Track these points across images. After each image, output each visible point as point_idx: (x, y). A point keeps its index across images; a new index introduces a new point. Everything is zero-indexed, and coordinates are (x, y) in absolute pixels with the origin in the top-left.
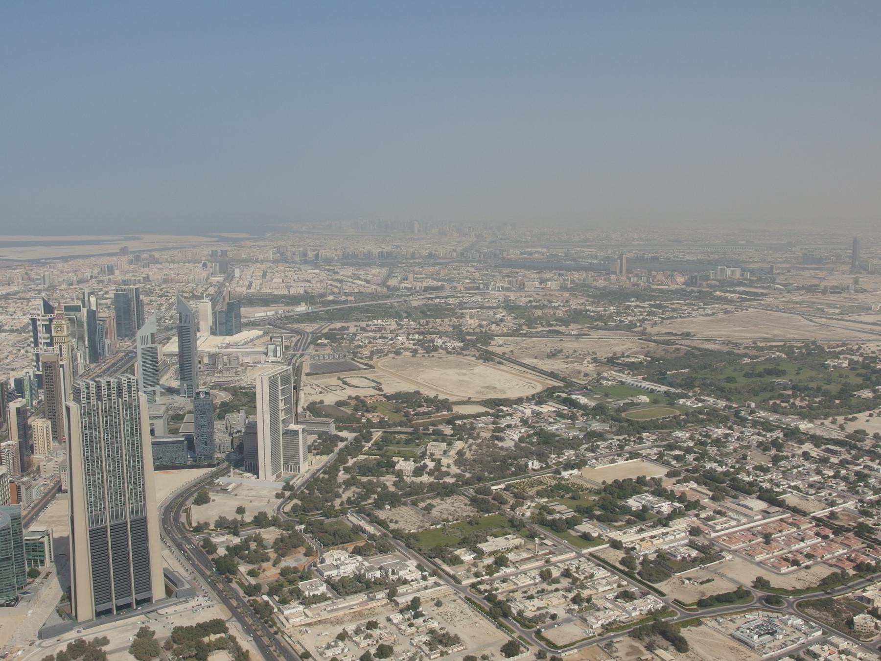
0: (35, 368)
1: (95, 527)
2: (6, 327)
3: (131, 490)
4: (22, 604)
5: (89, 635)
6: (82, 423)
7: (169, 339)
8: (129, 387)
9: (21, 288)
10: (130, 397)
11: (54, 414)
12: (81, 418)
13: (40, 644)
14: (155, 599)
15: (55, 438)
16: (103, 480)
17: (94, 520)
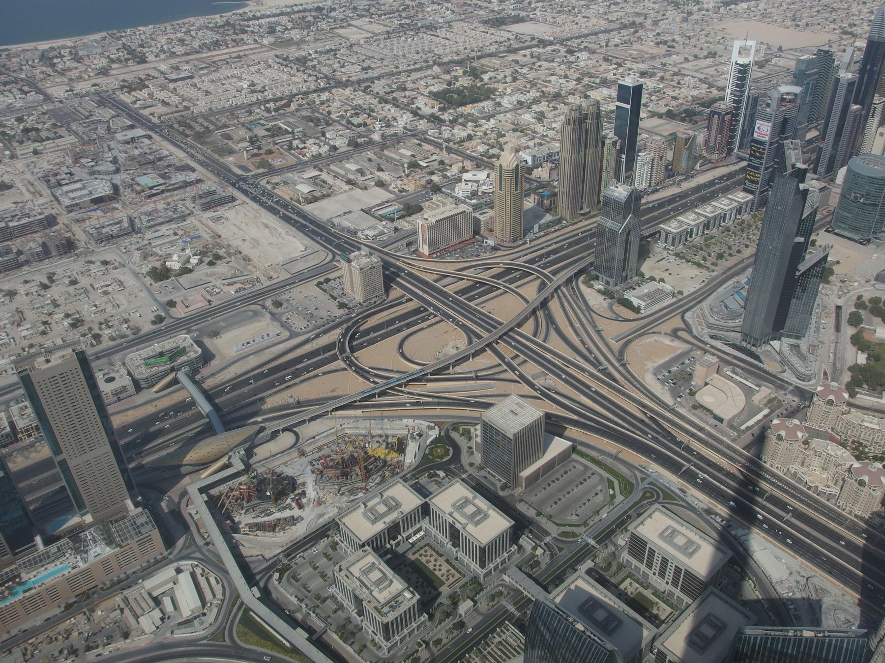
4: (871, 246)
13: (874, 285)
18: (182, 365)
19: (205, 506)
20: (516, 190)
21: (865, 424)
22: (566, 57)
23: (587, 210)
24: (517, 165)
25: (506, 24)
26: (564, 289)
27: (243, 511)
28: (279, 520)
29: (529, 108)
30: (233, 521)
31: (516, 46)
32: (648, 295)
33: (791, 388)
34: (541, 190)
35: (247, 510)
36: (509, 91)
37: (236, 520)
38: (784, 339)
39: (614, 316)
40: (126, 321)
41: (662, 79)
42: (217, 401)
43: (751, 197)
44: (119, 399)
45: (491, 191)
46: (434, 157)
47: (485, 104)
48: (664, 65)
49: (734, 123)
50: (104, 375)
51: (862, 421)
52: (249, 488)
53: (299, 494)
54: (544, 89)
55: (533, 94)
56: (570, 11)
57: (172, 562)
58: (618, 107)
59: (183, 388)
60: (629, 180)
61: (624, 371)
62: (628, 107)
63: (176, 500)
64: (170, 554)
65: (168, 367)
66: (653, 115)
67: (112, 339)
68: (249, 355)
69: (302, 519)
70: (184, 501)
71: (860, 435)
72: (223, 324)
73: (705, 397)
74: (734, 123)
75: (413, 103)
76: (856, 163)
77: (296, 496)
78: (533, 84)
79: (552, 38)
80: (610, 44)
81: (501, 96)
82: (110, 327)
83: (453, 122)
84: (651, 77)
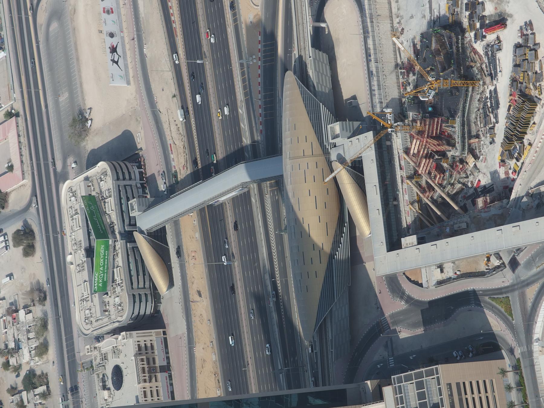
18: (123, 212)
19: (427, 247)
27: (471, 161)
28: (514, 81)
30: (486, 190)
35: (472, 151)
37: (485, 180)
40: (13, 310)
42: (220, 153)
44: (166, 368)
50: (105, 388)
52: (421, 133)
53: (471, 17)
57: (530, 354)
59: (176, 222)
63: (401, 305)
64: (511, 351)
65: (120, 244)
67: (42, 349)
68: (142, 56)
69: (529, 25)
70: (409, 289)
72: (64, 97)
77: (472, 27)
82: (18, 348)
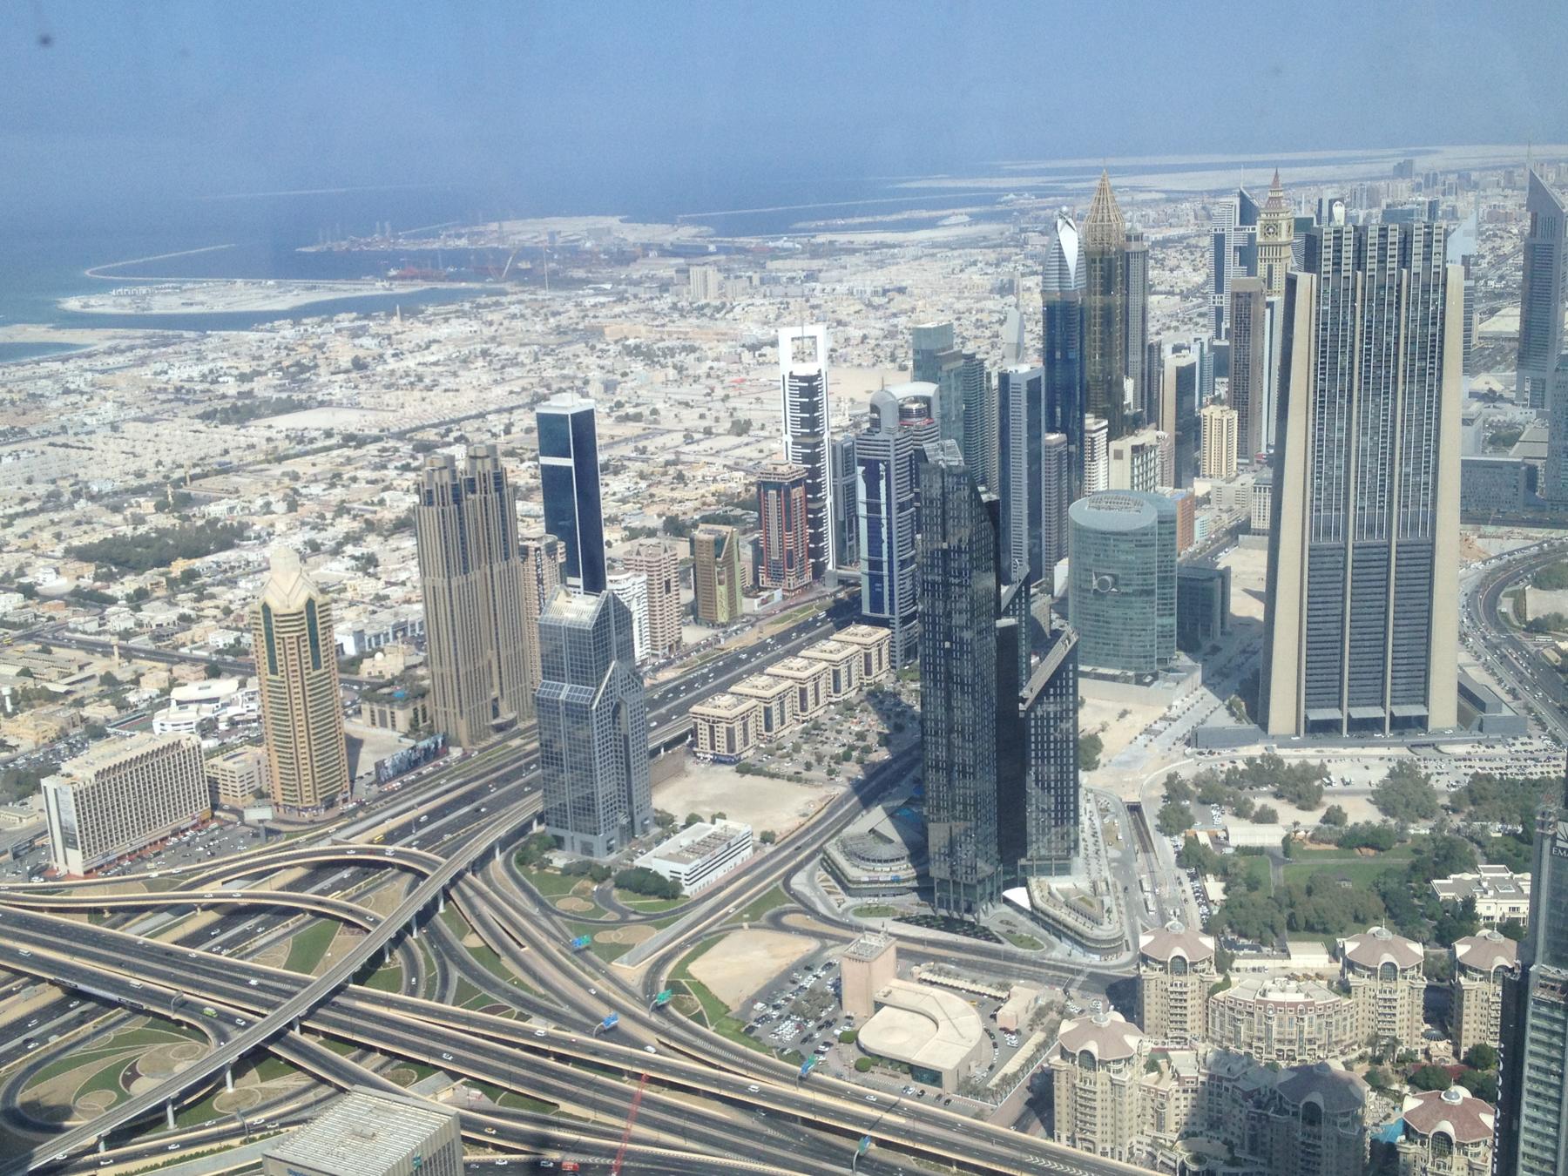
0: (1211, 333)
1: (1323, 542)
2: (1159, 288)
3: (1407, 475)
5: (1291, 757)
6: (1318, 314)
7: (1492, 312)
8: (1428, 246)
9: (1191, 230)
10: (1427, 269)
11: (1246, 403)
12: (1318, 303)
14: (1433, 724)
15: (1243, 452)
16: (1348, 472)
17: (1321, 527)
20: (317, 666)
21: (1274, 996)
22: (413, 457)
23: (511, 716)
24: (310, 603)
25: (258, 417)
26: (478, 881)
29: (336, 552)
31: (283, 445)
32: (696, 849)
33: (1081, 978)
34: (386, 690)
36: (280, 527)
38: (1033, 881)
39: (618, 916)
41: (642, 476)
43: (886, 631)
45: (253, 715)
46: (88, 672)
47: (222, 556)
48: (644, 451)
49: (811, 506)
51: (1264, 995)
54: (368, 516)
55: (345, 525)
56: (412, 384)
58: (546, 470)
60: (594, 583)
61: (666, 1025)
62: (569, 462)
66: (633, 534)
71: (1269, 1029)
73: (880, 1034)
74: (811, 506)
75: (24, 575)
76: (1081, 512)
78: (342, 510)
79: (375, 432)
80: (514, 430)
81: (263, 540)
83: (138, 599)
84: (616, 473)
